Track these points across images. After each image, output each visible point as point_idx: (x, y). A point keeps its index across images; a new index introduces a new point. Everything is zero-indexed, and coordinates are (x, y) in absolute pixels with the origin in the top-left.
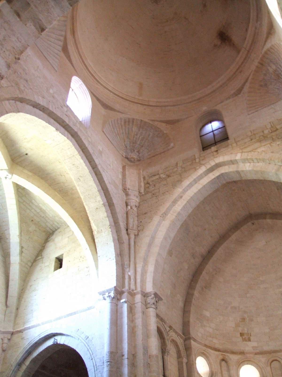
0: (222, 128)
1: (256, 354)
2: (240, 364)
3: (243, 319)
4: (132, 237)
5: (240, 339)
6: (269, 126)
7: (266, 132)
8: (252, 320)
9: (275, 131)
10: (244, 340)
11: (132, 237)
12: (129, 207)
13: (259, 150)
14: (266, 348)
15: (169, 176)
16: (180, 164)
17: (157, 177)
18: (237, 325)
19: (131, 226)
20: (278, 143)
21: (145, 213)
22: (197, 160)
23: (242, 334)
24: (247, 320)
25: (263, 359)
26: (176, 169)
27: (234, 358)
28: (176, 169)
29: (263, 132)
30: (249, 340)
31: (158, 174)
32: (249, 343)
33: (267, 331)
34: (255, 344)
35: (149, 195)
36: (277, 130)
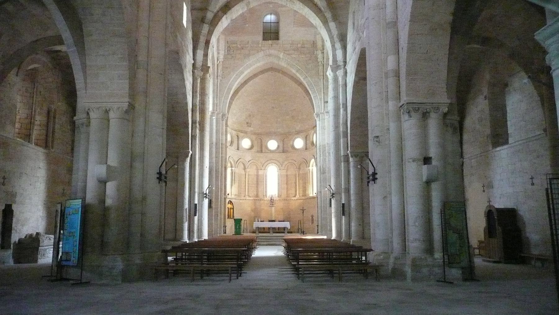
0: (275, 24)
1: (252, 134)
2: (243, 138)
3: (250, 116)
4: (219, 81)
5: (246, 126)
6: (301, 43)
7: (299, 45)
8: (254, 117)
9: (303, 47)
10: (248, 126)
11: (219, 81)
12: (218, 61)
13: (294, 56)
14: (257, 131)
15: (243, 49)
16: (250, 43)
17: (235, 45)
18: (246, 118)
19: (219, 74)
20: (303, 56)
21: (227, 68)
22: (260, 45)
23: (247, 123)
24: (252, 116)
25: (254, 137)
26: (247, 46)
27: (241, 135)
28: (247, 46)
29: (297, 45)
30: (250, 127)
31: (236, 44)
32: (250, 128)
33: (260, 123)
34: (252, 129)
35: (229, 57)
36: (305, 47)
